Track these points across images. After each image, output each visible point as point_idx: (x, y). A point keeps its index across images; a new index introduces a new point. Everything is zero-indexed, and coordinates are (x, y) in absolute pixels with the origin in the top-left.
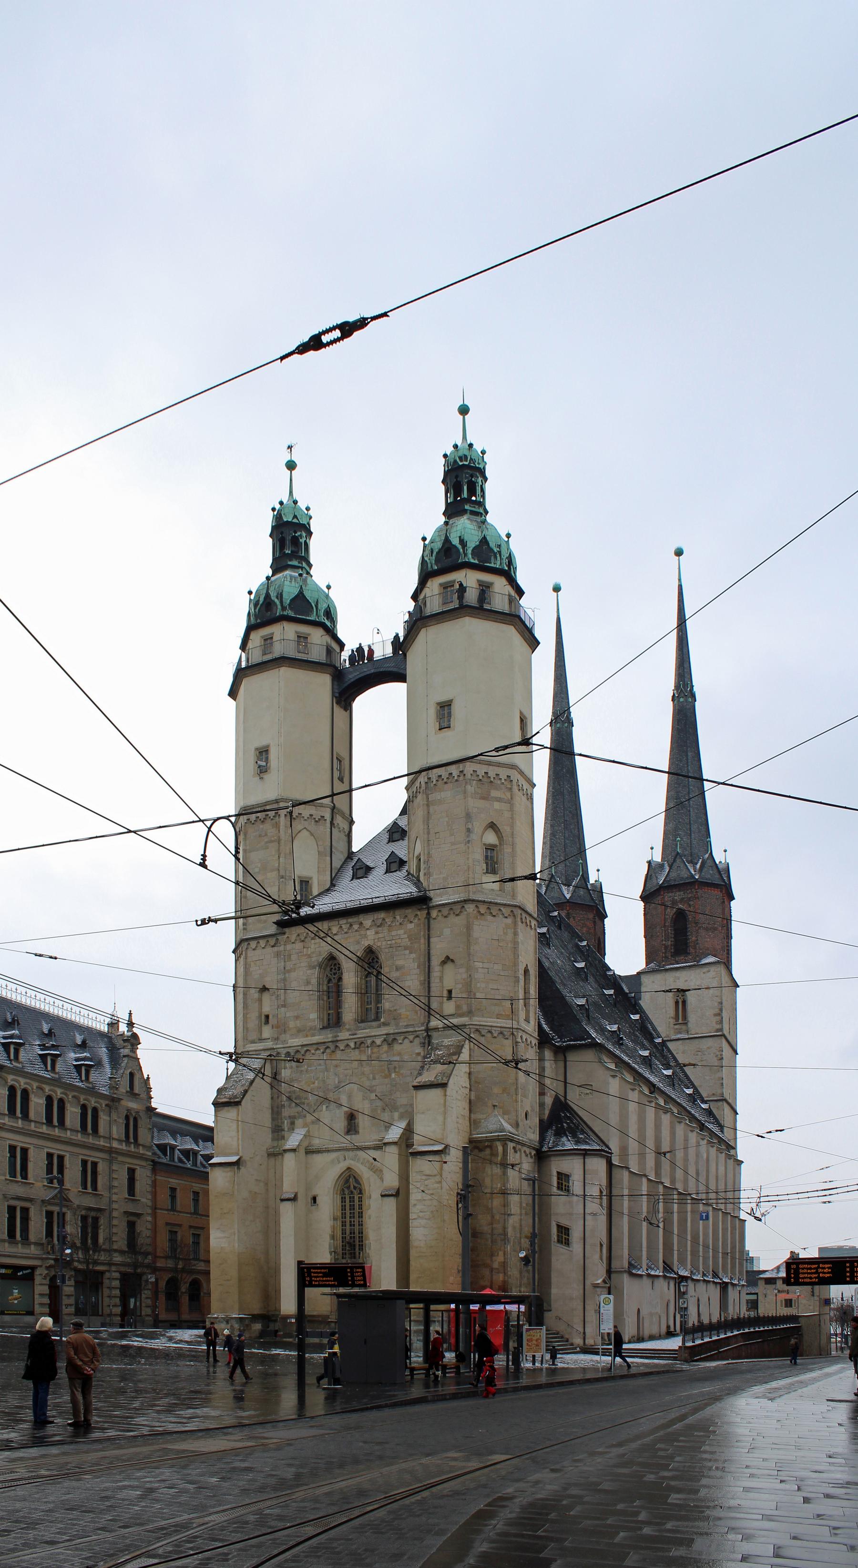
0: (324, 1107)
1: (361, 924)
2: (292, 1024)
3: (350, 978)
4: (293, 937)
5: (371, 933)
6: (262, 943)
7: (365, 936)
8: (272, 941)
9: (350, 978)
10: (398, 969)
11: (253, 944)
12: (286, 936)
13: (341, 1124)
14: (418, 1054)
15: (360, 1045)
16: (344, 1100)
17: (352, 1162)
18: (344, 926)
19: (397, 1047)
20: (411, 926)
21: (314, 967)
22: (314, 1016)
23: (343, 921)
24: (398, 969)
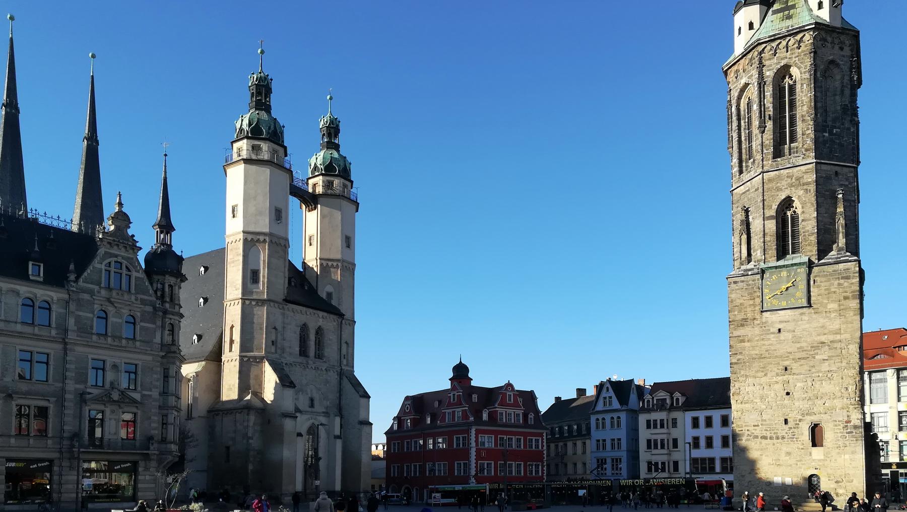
0: (301, 393)
1: (318, 315)
2: (288, 350)
3: (312, 337)
4: (290, 309)
5: (321, 320)
6: (276, 305)
7: (319, 321)
8: (281, 306)
9: (312, 337)
10: (330, 340)
11: (272, 304)
12: (288, 306)
13: (307, 402)
14: (336, 379)
15: (316, 369)
16: (309, 391)
17: (314, 421)
18: (312, 313)
19: (329, 374)
20: (335, 323)
21: (298, 326)
22: (298, 349)
23: (311, 310)
24: (330, 340)
